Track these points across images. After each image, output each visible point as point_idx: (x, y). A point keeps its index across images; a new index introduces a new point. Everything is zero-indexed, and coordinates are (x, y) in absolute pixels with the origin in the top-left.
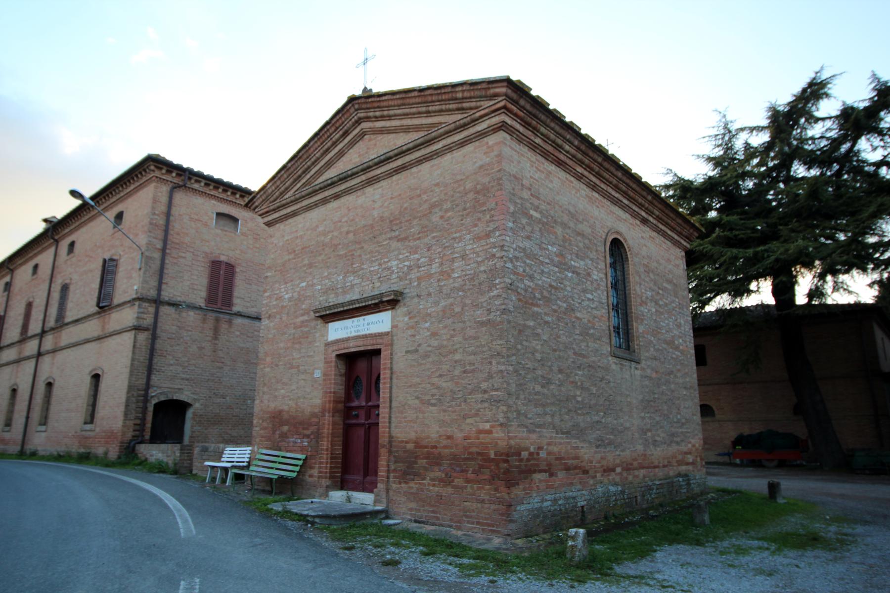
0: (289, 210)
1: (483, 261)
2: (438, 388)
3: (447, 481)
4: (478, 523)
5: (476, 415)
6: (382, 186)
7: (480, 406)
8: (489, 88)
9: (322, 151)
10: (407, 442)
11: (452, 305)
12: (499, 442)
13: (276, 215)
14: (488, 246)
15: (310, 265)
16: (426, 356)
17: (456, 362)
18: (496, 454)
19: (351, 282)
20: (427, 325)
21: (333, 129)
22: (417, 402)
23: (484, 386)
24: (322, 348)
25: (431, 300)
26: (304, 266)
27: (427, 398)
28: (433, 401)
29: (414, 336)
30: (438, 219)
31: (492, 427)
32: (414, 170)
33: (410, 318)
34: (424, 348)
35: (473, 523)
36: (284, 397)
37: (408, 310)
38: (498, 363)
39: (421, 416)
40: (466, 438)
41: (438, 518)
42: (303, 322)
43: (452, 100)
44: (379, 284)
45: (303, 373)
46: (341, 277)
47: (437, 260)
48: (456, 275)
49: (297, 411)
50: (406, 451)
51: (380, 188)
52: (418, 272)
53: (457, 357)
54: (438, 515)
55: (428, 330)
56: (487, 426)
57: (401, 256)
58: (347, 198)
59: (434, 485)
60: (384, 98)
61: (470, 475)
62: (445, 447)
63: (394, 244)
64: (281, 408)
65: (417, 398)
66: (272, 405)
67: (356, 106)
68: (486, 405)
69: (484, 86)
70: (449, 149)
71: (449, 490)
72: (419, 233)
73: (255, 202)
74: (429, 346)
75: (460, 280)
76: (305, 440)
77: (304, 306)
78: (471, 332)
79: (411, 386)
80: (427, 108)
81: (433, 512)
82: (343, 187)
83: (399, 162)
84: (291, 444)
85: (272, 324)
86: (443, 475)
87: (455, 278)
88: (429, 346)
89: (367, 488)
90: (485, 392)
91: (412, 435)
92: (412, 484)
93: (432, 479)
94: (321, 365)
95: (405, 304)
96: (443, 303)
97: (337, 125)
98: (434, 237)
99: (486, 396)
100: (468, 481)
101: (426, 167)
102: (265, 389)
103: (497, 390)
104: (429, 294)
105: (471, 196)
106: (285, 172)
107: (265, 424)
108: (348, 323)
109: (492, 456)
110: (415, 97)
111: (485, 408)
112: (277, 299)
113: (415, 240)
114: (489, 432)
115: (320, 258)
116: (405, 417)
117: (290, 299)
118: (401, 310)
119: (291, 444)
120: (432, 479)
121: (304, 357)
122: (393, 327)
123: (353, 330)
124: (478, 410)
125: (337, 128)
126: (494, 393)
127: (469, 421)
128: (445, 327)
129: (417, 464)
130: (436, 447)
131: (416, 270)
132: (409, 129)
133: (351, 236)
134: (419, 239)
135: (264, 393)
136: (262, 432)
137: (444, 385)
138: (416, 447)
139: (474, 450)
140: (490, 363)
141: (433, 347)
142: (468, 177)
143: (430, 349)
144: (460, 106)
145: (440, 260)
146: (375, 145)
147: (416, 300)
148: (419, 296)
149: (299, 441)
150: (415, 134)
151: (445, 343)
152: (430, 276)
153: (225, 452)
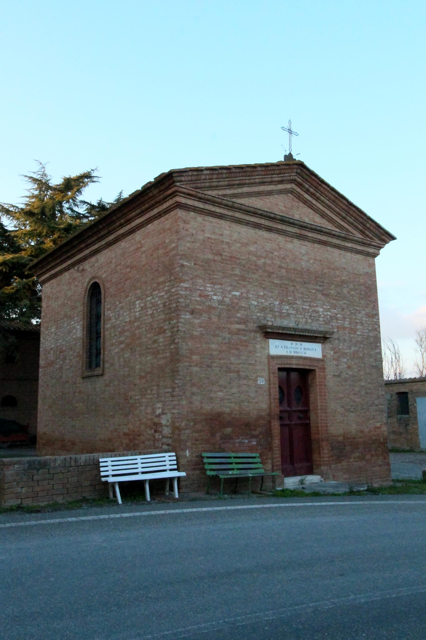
0: (218, 210)
1: (371, 330)
2: (354, 401)
3: (362, 458)
4: (380, 478)
5: (374, 418)
6: (307, 246)
7: (375, 413)
8: (384, 235)
9: (261, 180)
10: (339, 436)
11: (358, 351)
12: (384, 433)
13: (200, 205)
14: (373, 323)
15: (243, 278)
16: (346, 380)
17: (362, 386)
18: (383, 440)
19: (287, 310)
20: (345, 360)
21: (277, 172)
22: (343, 409)
23: (376, 402)
24: (266, 361)
25: (346, 344)
26: (236, 275)
27: (349, 407)
28: (352, 410)
29: (337, 365)
30: (346, 292)
31: (381, 425)
32: (329, 248)
33: (334, 353)
34: (344, 375)
35: (378, 479)
36: (222, 400)
37: (332, 347)
38: (381, 390)
39: (346, 419)
40: (370, 432)
41: (361, 480)
42: (239, 330)
43: (362, 224)
44: (310, 321)
45: (245, 379)
46: (277, 303)
47: (348, 320)
48: (359, 334)
49: (241, 414)
50: (338, 442)
51: (305, 245)
52: (337, 322)
53: (363, 384)
54: (361, 479)
55: (346, 363)
56: (379, 425)
57: (325, 307)
58: (276, 236)
59: (356, 461)
60: (324, 186)
61: (373, 453)
62: (360, 438)
63: (320, 296)
64: (220, 410)
65: (342, 407)
66: (208, 407)
67: (299, 171)
68: (378, 413)
69: (382, 231)
70: (351, 250)
71: (364, 462)
72: (336, 296)
73: (182, 176)
74: (347, 374)
75: (361, 337)
76: (252, 440)
77: (239, 315)
78: (368, 371)
79: (337, 399)
80: (346, 216)
81: (358, 477)
82: (280, 227)
83: (324, 238)
84: (237, 445)
85: (197, 321)
86: (360, 454)
87: (358, 335)
88: (347, 374)
89: (310, 471)
90: (377, 406)
91: (341, 432)
92: (344, 463)
93: (354, 458)
94: (266, 374)
95: (330, 342)
96: (353, 349)
97: (282, 171)
98: (345, 303)
99: (377, 408)
100: (372, 456)
101: (336, 252)
102: (194, 389)
103: (382, 405)
104: (345, 340)
105: (363, 287)
106: (227, 173)
107: (199, 427)
108: (288, 343)
109: (382, 440)
110: (344, 204)
111: (377, 415)
112: (200, 296)
113: (334, 299)
114: (379, 428)
115: (254, 276)
116: (336, 420)
117: (221, 302)
118: (328, 346)
119: (237, 445)
120: (354, 458)
121: (244, 364)
122: (324, 356)
123: (292, 350)
124: (374, 416)
125: (280, 174)
126: (381, 407)
127: (371, 422)
128: (355, 364)
129: (345, 449)
130: (355, 438)
131: (335, 321)
132: (326, 217)
133: (284, 271)
134: (336, 300)
135: (193, 394)
136: (195, 434)
137: (357, 400)
138: (344, 439)
139: (374, 438)
140: (378, 390)
141: (349, 375)
142: (361, 275)
143: (347, 376)
144: (364, 230)
145: (349, 320)
146: (298, 208)
147: (337, 341)
148: (339, 340)
149: (246, 441)
150: (327, 223)
151: (356, 374)
152: (344, 328)
153: (101, 464)
